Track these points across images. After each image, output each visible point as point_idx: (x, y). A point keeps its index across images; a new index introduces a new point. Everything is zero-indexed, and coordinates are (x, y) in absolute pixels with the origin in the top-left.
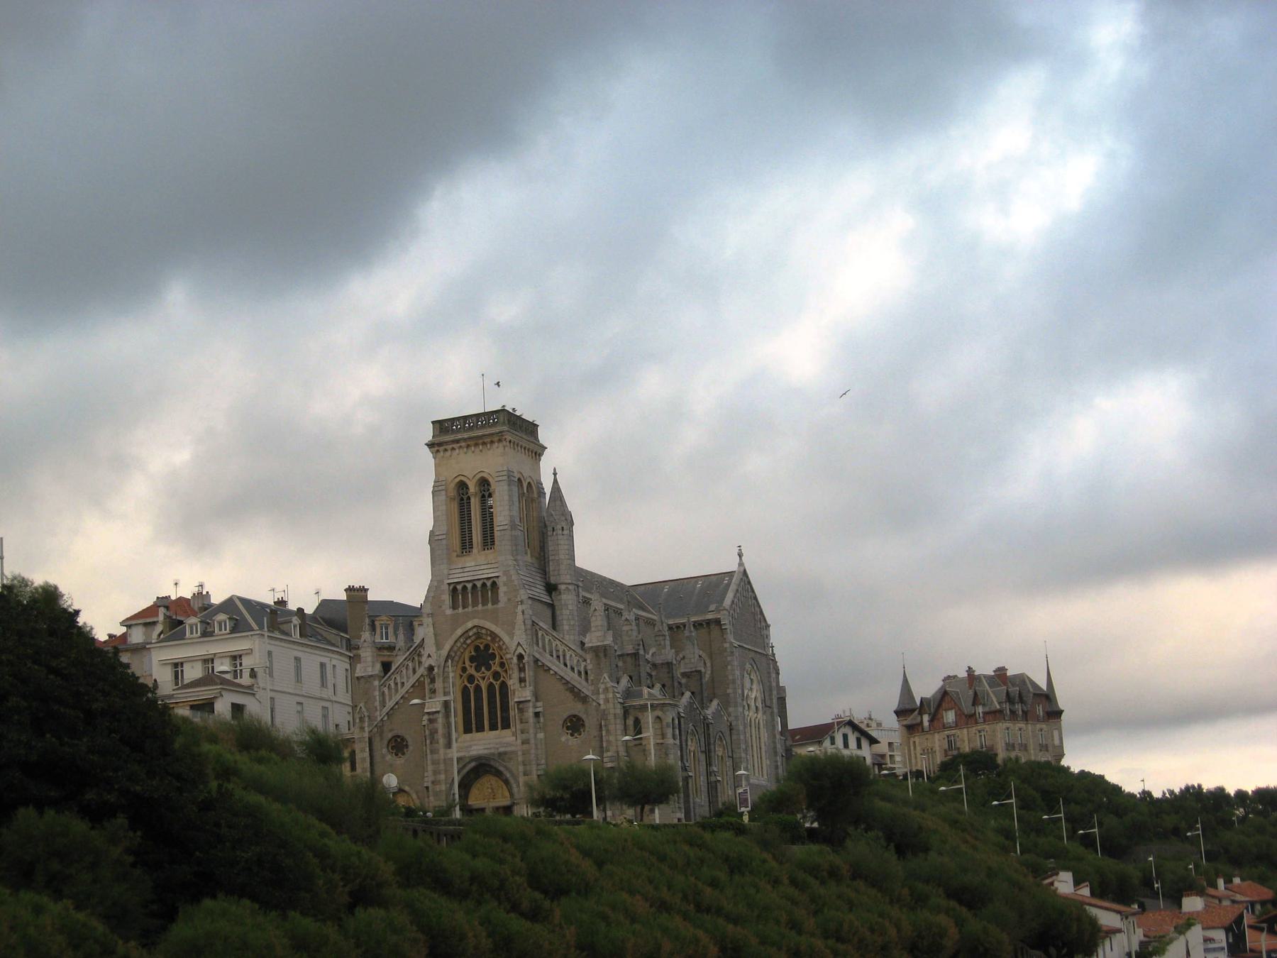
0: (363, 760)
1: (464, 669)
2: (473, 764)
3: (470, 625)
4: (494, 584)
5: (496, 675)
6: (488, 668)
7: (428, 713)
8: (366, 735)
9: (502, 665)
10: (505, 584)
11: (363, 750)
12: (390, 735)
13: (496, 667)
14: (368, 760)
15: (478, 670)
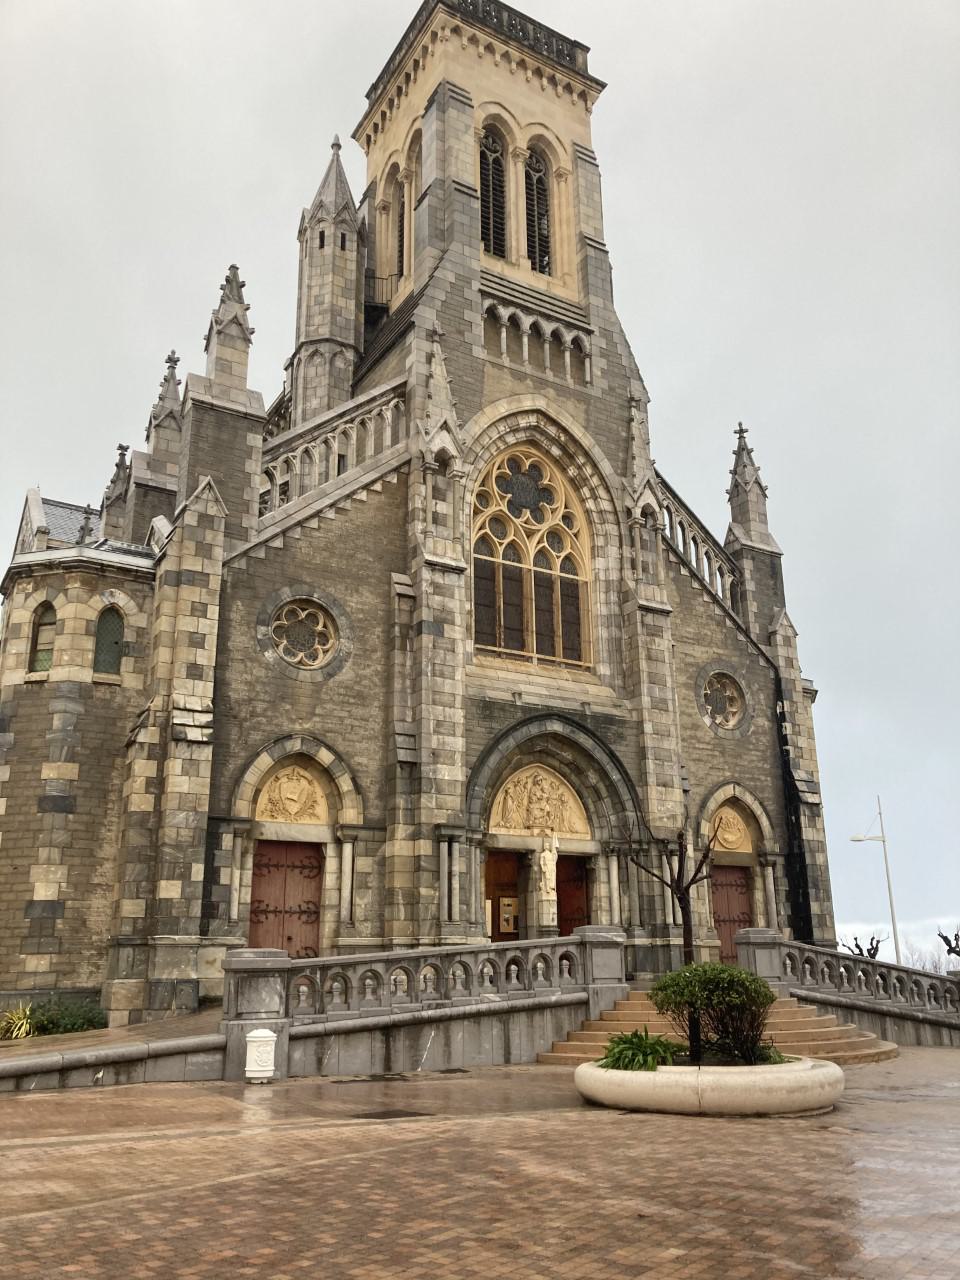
0: (197, 641)
1: (483, 497)
2: (534, 729)
3: (527, 404)
4: (576, 341)
5: (554, 536)
6: (539, 516)
7: (431, 565)
8: (215, 571)
9: (568, 519)
10: (603, 354)
11: (199, 610)
12: (286, 594)
13: (553, 520)
14: (212, 642)
15: (516, 508)
